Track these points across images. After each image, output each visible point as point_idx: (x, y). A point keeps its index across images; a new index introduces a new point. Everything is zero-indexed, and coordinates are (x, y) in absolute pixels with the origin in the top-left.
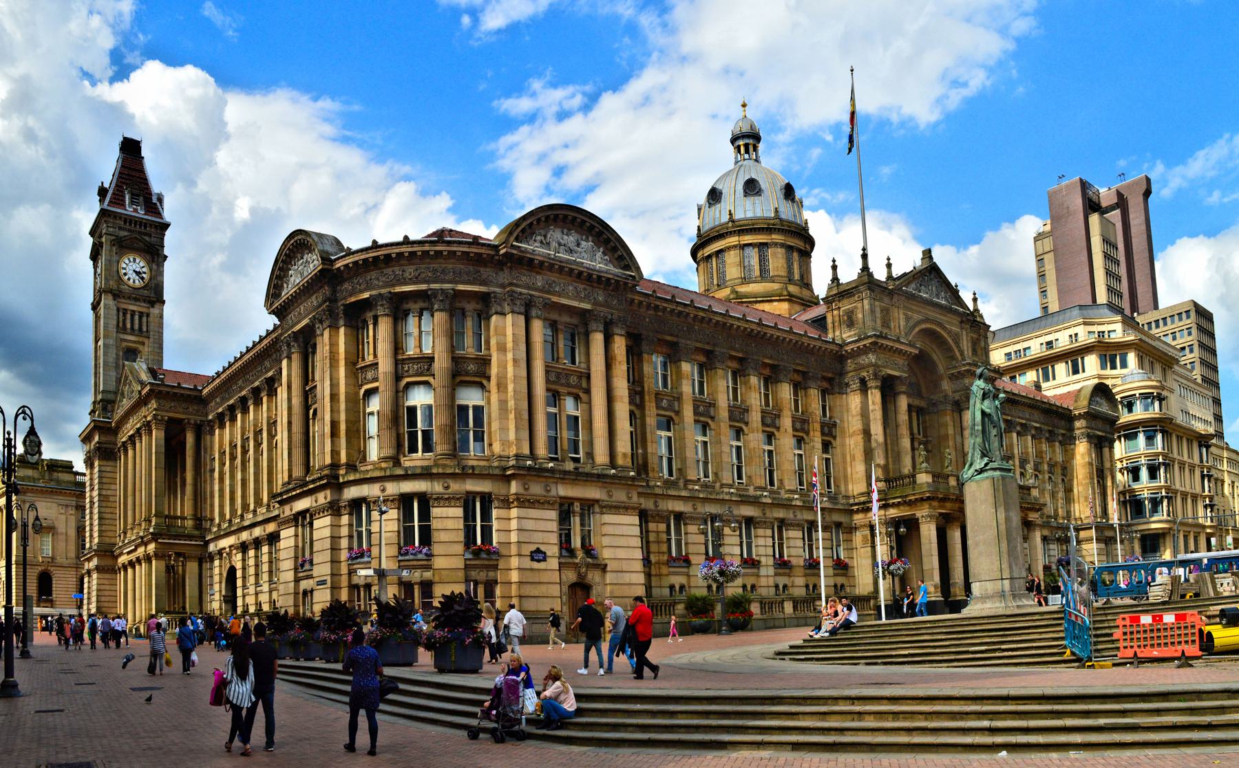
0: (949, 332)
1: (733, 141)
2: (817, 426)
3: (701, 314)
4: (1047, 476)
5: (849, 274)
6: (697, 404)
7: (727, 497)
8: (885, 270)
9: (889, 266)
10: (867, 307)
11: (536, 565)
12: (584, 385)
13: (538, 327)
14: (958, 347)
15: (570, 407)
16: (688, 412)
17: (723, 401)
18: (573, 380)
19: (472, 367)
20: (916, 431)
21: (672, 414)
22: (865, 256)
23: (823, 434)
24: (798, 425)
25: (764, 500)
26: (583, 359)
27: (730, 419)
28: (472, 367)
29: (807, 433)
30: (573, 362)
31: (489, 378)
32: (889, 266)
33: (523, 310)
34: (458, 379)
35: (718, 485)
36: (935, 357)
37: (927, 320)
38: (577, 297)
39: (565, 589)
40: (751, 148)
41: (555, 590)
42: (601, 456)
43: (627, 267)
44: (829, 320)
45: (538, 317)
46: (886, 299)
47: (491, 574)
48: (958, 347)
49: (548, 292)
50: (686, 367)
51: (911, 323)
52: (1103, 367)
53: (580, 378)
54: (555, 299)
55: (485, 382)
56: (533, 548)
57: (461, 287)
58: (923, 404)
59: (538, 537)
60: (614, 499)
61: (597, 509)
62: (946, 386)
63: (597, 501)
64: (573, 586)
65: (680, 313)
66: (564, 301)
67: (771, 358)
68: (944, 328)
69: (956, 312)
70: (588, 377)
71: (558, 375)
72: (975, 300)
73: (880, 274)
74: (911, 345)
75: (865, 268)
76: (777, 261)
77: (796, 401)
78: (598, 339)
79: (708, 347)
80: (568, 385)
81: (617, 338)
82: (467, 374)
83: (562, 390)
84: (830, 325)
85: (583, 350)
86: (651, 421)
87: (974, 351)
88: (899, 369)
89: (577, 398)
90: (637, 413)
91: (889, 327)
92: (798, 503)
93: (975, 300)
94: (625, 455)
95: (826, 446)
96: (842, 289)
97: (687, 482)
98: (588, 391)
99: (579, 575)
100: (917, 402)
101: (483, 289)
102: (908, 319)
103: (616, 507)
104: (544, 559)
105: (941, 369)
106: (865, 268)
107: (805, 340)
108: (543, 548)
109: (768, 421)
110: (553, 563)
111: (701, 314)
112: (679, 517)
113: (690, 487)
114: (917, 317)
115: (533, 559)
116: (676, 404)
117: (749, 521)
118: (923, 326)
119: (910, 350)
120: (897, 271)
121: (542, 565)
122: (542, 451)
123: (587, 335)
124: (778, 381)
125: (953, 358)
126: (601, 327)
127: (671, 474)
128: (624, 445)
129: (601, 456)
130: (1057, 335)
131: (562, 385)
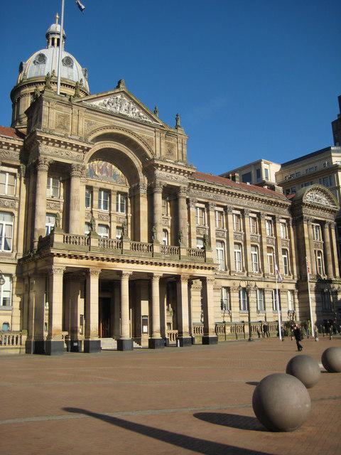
46: (64, 108)
51: (94, 127)
88: (72, 159)
100: (119, 189)
102: (90, 124)
105: (138, 164)
118: (109, 131)
125: (146, 156)
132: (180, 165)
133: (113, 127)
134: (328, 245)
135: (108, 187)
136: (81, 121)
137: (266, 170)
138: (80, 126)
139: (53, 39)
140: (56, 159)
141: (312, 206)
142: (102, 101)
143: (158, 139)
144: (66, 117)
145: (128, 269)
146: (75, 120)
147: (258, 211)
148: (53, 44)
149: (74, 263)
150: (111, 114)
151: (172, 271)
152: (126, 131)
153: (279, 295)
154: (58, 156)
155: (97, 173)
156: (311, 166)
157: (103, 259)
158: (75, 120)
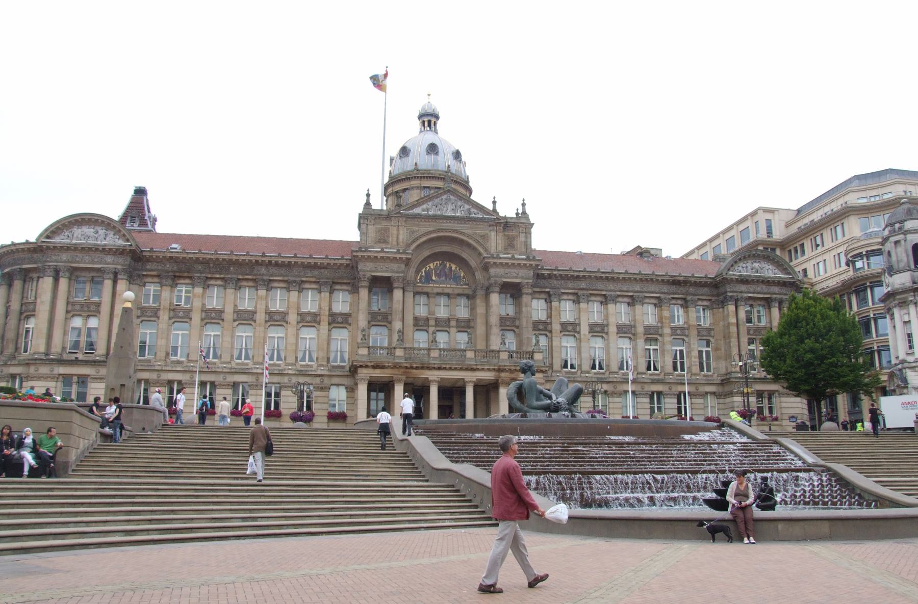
0: (468, 236)
1: (421, 116)
13: (63, 283)
22: (368, 195)
43: (128, 240)
49: (71, 262)
57: (24, 266)
62: (479, 275)
68: (461, 233)
78: (108, 283)
81: (119, 281)
88: (393, 271)
92: (290, 372)
105: (473, 263)
114: (424, 230)
119: (404, 256)
132: (519, 259)
133: (439, 230)
136: (401, 232)
138: (401, 237)
139: (429, 122)
140: (374, 274)
142: (424, 206)
143: (493, 234)
146: (395, 232)
147: (658, 295)
148: (429, 125)
149: (378, 373)
150: (435, 218)
151: (488, 376)
153: (659, 402)
154: (377, 271)
155: (434, 278)
157: (406, 368)
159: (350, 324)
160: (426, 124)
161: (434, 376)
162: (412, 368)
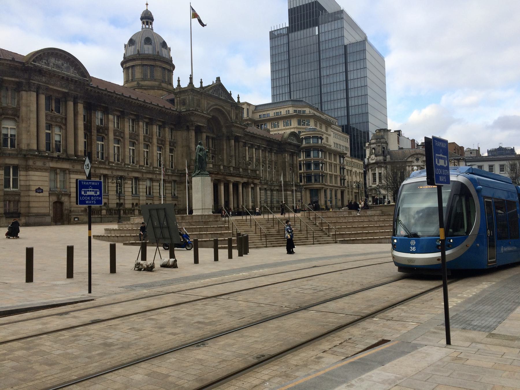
2: (168, 143)
3: (119, 96)
4: (268, 166)
5: (184, 84)
6: (115, 132)
7: (127, 169)
8: (200, 84)
9: (201, 83)
10: (190, 98)
11: (38, 194)
12: (64, 121)
14: (229, 115)
15: (57, 130)
16: (111, 136)
17: (127, 131)
18: (59, 120)
19: (10, 112)
20: (211, 146)
21: (104, 135)
22: (191, 78)
23: (170, 145)
24: (160, 142)
25: (143, 171)
26: (64, 111)
27: (130, 138)
28: (10, 112)
29: (164, 145)
30: (59, 112)
31: (18, 117)
32: (201, 83)
33: (36, 90)
34: (3, 116)
35: (123, 164)
36: (220, 119)
37: (216, 105)
38: (61, 86)
39: (51, 204)
40: (149, 24)
41: (47, 204)
42: (71, 151)
44: (176, 101)
45: (43, 94)
47: (17, 198)
48: (229, 115)
49: (48, 84)
50: (111, 117)
51: (209, 106)
52: (299, 124)
53: (62, 119)
54: (51, 87)
55: (16, 118)
56: (37, 187)
58: (214, 136)
59: (40, 183)
60: (75, 168)
61: (67, 172)
62: (224, 130)
63: (68, 169)
64: (55, 203)
65: (109, 95)
66: (55, 88)
67: (149, 115)
69: (228, 102)
70: (66, 119)
71: (52, 118)
72: (238, 98)
73: (197, 85)
74: (208, 114)
75: (191, 83)
76: (158, 74)
77: (159, 133)
78: (71, 104)
79: (121, 110)
80: (56, 122)
81: (79, 104)
82: (7, 114)
83: (53, 123)
84: (176, 104)
85: (64, 107)
86: (94, 137)
87: (237, 117)
89: (60, 127)
90: (88, 134)
91: (200, 107)
93: (238, 98)
94: (81, 151)
95: (171, 151)
96: (181, 90)
97: (109, 162)
98: (65, 125)
99: (58, 198)
100: (212, 135)
101: (17, 80)
102: (208, 104)
103: (76, 172)
104: (42, 192)
105: (222, 123)
106: (191, 83)
107: (164, 109)
108: (41, 188)
109: (147, 140)
110: (46, 194)
111: (119, 96)
112: (105, 176)
113: (111, 164)
114: (212, 103)
115: (36, 192)
116: (106, 131)
117: (137, 179)
118: (215, 107)
120: (204, 85)
121: (41, 194)
122: (43, 147)
123: (66, 102)
124: (152, 124)
126: (72, 100)
127: (102, 158)
128: (81, 147)
129: (71, 151)
130: (282, 110)
131: (53, 121)
134: (295, 165)
135: (208, 135)
137: (248, 109)
141: (290, 144)
144: (200, 100)
145: (233, 179)
151: (245, 180)
152: (221, 106)
156: (278, 111)
158: (203, 102)
159: (175, 147)
160: (145, 23)
161: (233, 179)
162: (227, 176)
